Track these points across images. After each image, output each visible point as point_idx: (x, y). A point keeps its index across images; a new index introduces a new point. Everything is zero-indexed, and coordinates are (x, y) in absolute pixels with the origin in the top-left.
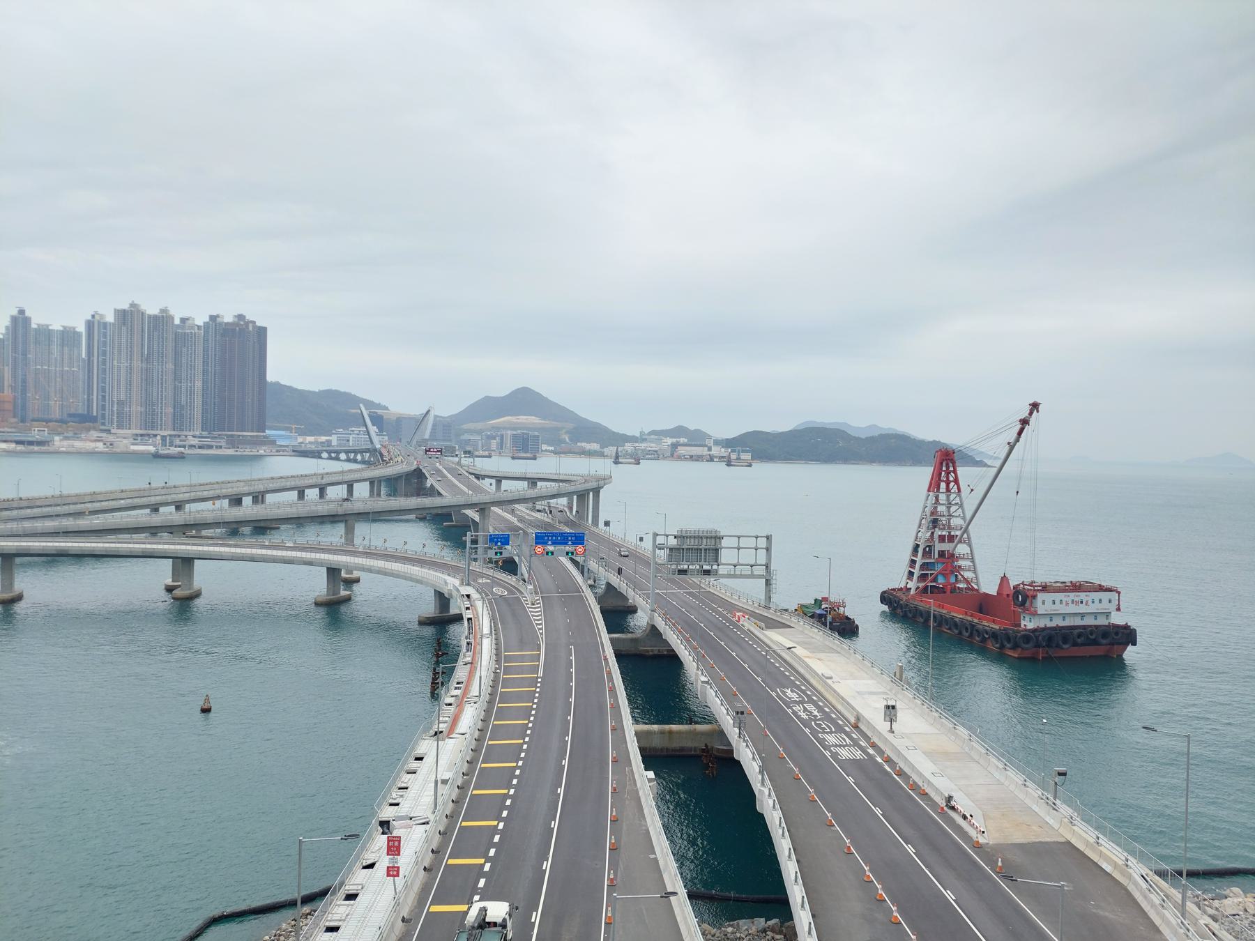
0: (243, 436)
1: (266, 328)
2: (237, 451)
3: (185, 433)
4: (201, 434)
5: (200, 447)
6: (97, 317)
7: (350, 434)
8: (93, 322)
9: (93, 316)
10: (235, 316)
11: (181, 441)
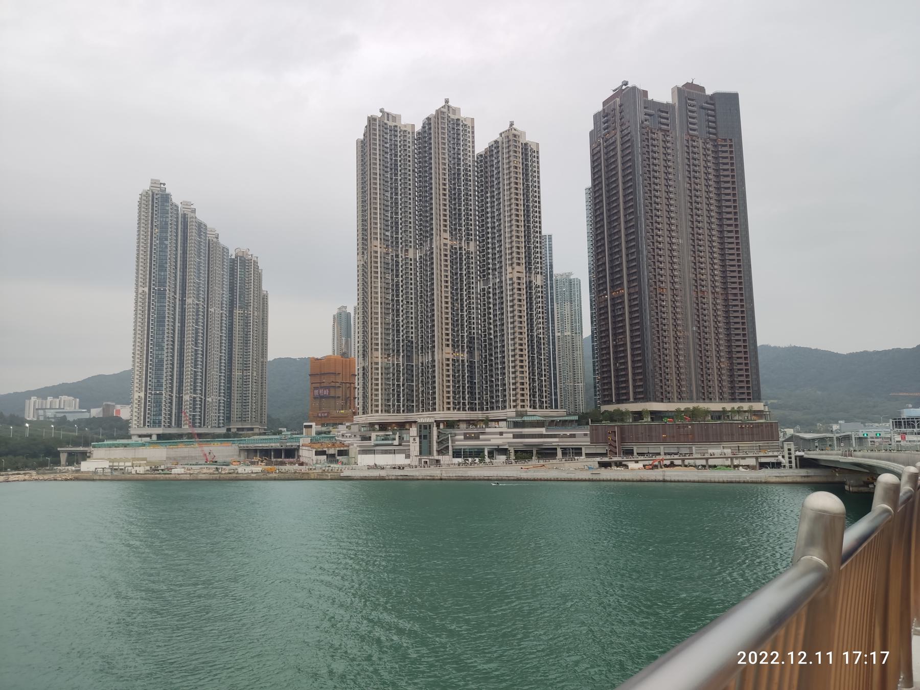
0: (656, 415)
3: (493, 414)
4: (520, 414)
5: (523, 454)
11: (467, 437)
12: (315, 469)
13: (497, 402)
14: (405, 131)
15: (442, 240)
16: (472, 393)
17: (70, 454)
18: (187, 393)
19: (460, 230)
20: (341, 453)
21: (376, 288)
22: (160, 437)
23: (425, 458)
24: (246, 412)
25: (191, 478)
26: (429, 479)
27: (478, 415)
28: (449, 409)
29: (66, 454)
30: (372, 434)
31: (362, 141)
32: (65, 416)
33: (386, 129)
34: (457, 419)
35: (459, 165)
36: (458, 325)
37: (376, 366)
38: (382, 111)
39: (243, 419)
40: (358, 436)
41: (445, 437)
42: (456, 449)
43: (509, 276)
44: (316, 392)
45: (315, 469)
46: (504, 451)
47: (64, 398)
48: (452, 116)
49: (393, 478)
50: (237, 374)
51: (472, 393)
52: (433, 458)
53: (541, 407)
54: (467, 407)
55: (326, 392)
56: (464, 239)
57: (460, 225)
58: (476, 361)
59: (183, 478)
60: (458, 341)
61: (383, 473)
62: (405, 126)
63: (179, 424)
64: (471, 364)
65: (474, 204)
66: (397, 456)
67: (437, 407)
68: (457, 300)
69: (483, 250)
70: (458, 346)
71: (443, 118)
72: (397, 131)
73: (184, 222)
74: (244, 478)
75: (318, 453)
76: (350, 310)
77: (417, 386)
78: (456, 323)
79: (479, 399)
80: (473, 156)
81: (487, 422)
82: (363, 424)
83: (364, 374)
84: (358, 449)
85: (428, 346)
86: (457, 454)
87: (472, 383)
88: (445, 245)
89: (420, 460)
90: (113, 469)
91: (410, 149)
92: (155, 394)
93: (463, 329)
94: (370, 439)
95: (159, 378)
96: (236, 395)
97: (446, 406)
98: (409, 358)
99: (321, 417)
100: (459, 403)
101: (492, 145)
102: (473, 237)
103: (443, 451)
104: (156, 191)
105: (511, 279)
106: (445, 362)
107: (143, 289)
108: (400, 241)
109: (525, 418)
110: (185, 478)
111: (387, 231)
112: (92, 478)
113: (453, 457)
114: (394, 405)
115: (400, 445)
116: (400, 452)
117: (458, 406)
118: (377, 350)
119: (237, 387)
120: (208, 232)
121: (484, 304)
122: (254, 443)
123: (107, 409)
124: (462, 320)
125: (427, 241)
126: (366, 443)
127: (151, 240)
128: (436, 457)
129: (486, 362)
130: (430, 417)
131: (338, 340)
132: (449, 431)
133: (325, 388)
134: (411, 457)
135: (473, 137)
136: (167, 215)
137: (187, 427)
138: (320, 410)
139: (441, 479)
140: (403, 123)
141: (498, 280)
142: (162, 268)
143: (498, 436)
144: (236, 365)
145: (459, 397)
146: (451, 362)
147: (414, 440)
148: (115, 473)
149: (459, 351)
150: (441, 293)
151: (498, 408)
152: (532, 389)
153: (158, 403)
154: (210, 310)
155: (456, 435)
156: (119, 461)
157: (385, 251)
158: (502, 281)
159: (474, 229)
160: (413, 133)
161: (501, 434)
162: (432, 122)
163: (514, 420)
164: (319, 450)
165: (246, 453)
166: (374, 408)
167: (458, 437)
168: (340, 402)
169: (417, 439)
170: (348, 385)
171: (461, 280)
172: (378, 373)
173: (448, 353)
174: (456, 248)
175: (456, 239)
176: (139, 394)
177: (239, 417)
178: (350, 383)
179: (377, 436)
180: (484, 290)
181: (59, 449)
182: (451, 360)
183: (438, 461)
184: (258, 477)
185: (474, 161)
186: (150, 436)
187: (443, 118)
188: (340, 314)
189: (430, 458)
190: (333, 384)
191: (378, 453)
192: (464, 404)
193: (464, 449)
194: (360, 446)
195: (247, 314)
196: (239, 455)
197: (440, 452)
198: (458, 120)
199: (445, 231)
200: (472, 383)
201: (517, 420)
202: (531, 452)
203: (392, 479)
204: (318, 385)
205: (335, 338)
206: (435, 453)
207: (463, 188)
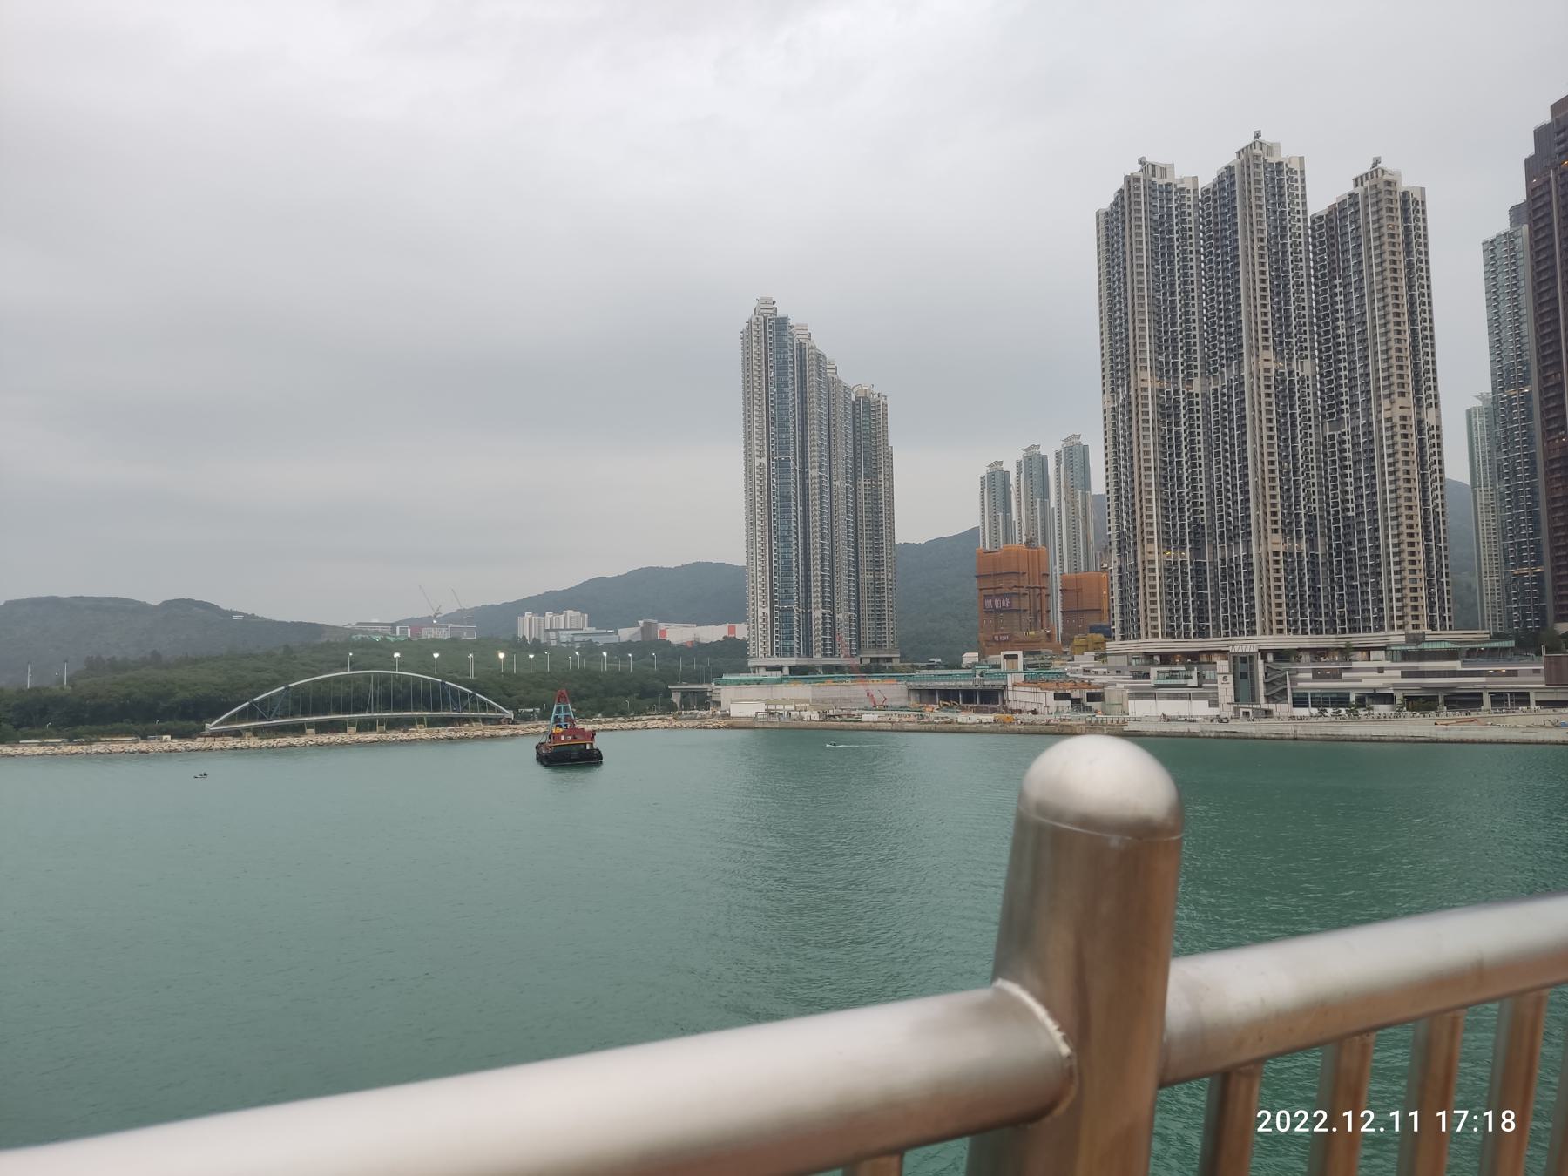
3: (1358, 639)
5: (1421, 703)
11: (1318, 675)
12: (1070, 720)
13: (1366, 619)
14: (1183, 189)
15: (1259, 362)
16: (1315, 606)
17: (685, 693)
18: (818, 608)
19: (1289, 343)
20: (1093, 697)
21: (1146, 445)
22: (793, 670)
23: (1244, 707)
24: (881, 633)
25: (894, 728)
26: (1274, 739)
27: (1327, 640)
28: (1280, 631)
29: (680, 693)
30: (1152, 669)
31: (1106, 213)
32: (591, 640)
33: (1154, 191)
34: (1296, 647)
35: (1283, 237)
36: (1289, 497)
37: (1151, 566)
38: (1142, 162)
39: (878, 644)
40: (1127, 672)
41: (1279, 676)
42: (1298, 694)
43: (1384, 415)
44: (989, 603)
45: (1070, 720)
46: (1388, 698)
47: (570, 613)
48: (1270, 160)
49: (1212, 735)
50: (866, 577)
51: (1315, 606)
52: (1259, 706)
53: (1443, 627)
54: (1309, 627)
55: (1005, 603)
56: (1295, 356)
57: (1289, 335)
58: (1319, 553)
59: (881, 728)
60: (1290, 523)
61: (1194, 728)
62: (1182, 181)
63: (808, 653)
64: (1313, 557)
65: (1308, 297)
66: (1195, 703)
67: (1258, 628)
68: (1287, 456)
69: (1329, 374)
70: (1291, 531)
71: (1257, 166)
72: (1170, 192)
73: (801, 356)
74: (973, 730)
75: (1057, 697)
76: (1010, 468)
77: (1215, 595)
78: (1289, 495)
79: (1327, 614)
80: (1305, 220)
81: (1346, 652)
82: (1133, 654)
83: (1120, 577)
84: (1128, 692)
85: (1235, 529)
86: (1299, 701)
87: (1314, 589)
88: (1267, 370)
89: (1236, 710)
90: (770, 713)
91: (1192, 218)
92: (783, 610)
93: (1297, 503)
94: (1147, 676)
95: (786, 587)
96: (866, 610)
97: (1275, 627)
98: (1197, 550)
99: (999, 641)
100: (1295, 622)
101: (1344, 201)
102: (1308, 352)
103: (1276, 696)
104: (768, 314)
105: (1389, 420)
106: (1272, 558)
107: (760, 461)
108: (1181, 368)
109: (1425, 646)
110: (885, 728)
111: (1160, 354)
112: (751, 725)
113: (1294, 706)
114: (1179, 626)
115: (1200, 686)
116: (1199, 697)
117: (1296, 627)
118: (1151, 541)
119: (868, 597)
120: (828, 367)
121: (1334, 462)
122: (931, 681)
123: (647, 629)
124: (1297, 489)
125: (1229, 366)
126: (1142, 683)
127: (767, 388)
128: (1266, 706)
129: (1339, 555)
130: (1251, 644)
131: (990, 516)
132: (1284, 666)
133: (1002, 596)
134: (1220, 705)
135: (1304, 188)
136: (786, 349)
137: (819, 656)
138: (995, 631)
139: (1295, 739)
140: (1177, 176)
141: (1362, 422)
142: (783, 428)
143: (1376, 674)
144: (865, 564)
145: (1296, 613)
146: (1281, 557)
147: (1225, 679)
148: (772, 719)
149: (1292, 539)
150: (1259, 446)
151: (1366, 629)
152: (1430, 596)
153: (788, 622)
154: (834, 483)
155: (1298, 672)
156: (776, 702)
157: (1157, 385)
158: (1371, 424)
159: (1311, 338)
160: (1195, 191)
161: (1381, 670)
162: (1236, 172)
163: (1403, 648)
164: (1060, 692)
165: (918, 695)
166: (1150, 631)
167: (1301, 676)
168: (1027, 618)
169: (1230, 678)
170: (1038, 591)
171: (1293, 425)
172: (1154, 577)
173: (1277, 542)
174: (1282, 374)
175: (1283, 358)
176: (764, 610)
177: (873, 642)
178: (1041, 588)
179: (1159, 672)
180: (1331, 438)
181: (670, 687)
182: (1281, 554)
183: (1268, 713)
184: (992, 730)
185: (1306, 227)
186: (780, 669)
187: (1257, 166)
188: (992, 476)
189: (1255, 706)
190: (1015, 590)
191: (1160, 699)
192: (1303, 623)
193: (1311, 694)
194: (1132, 688)
195: (876, 486)
196: (909, 699)
197: (1269, 699)
198: (1280, 164)
199: (1266, 348)
200: (1314, 589)
201: (1408, 648)
202: (1435, 699)
203: (1210, 737)
204: (991, 592)
205: (986, 516)
206: (1262, 700)
207: (1291, 274)
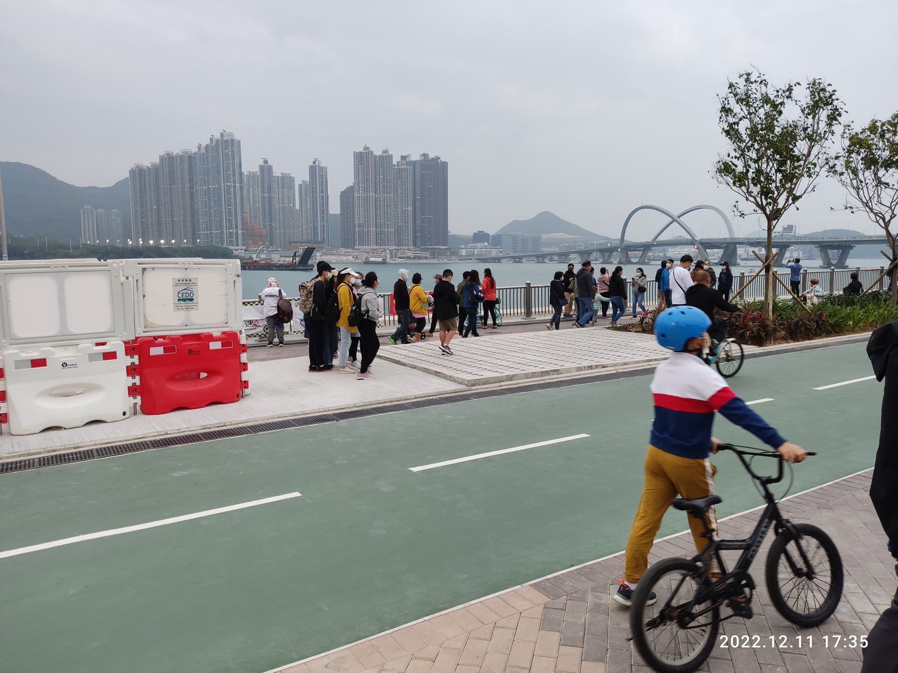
1: (447, 163)
2: (438, 260)
3: (402, 247)
5: (414, 258)
6: (317, 163)
7: (475, 249)
8: (315, 167)
9: (314, 162)
10: (422, 155)
183: (395, 260)
